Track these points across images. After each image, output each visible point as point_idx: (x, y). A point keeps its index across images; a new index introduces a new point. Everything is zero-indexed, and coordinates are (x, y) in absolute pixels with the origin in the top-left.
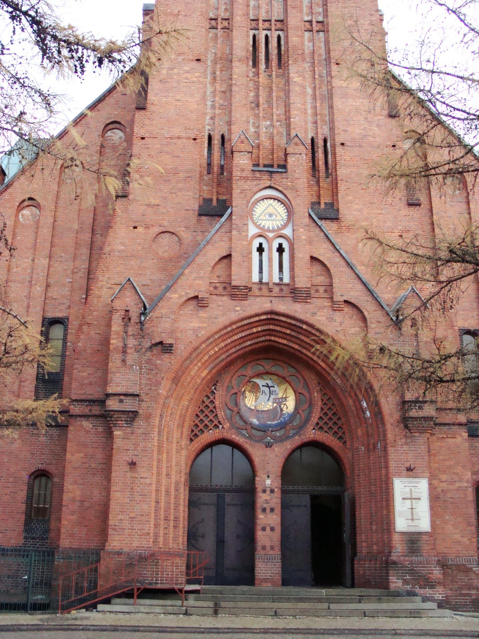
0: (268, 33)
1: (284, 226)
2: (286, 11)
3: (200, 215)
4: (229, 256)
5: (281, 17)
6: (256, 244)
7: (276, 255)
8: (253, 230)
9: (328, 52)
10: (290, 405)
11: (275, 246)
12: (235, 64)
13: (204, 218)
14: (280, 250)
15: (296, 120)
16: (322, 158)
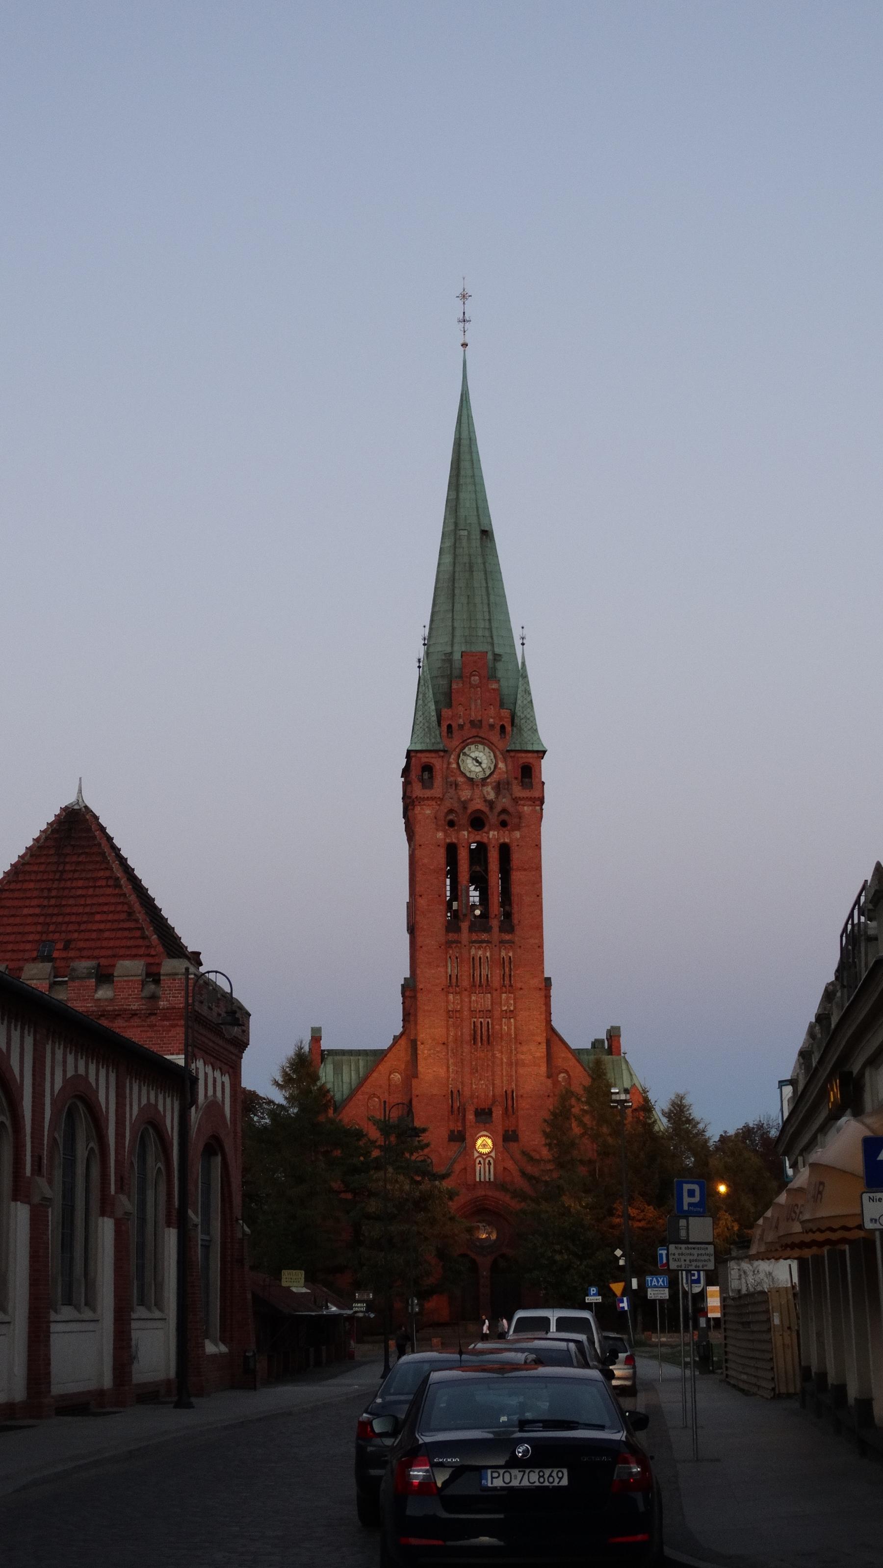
0: (482, 1020)
1: (491, 1152)
2: (492, 1004)
3: (450, 1140)
4: (465, 1169)
5: (490, 1008)
6: (477, 1161)
7: (487, 1166)
8: (476, 1155)
9: (516, 1035)
10: (494, 1237)
11: (487, 1162)
12: (465, 1046)
13: (452, 1143)
14: (489, 1163)
15: (498, 1082)
16: (509, 1100)
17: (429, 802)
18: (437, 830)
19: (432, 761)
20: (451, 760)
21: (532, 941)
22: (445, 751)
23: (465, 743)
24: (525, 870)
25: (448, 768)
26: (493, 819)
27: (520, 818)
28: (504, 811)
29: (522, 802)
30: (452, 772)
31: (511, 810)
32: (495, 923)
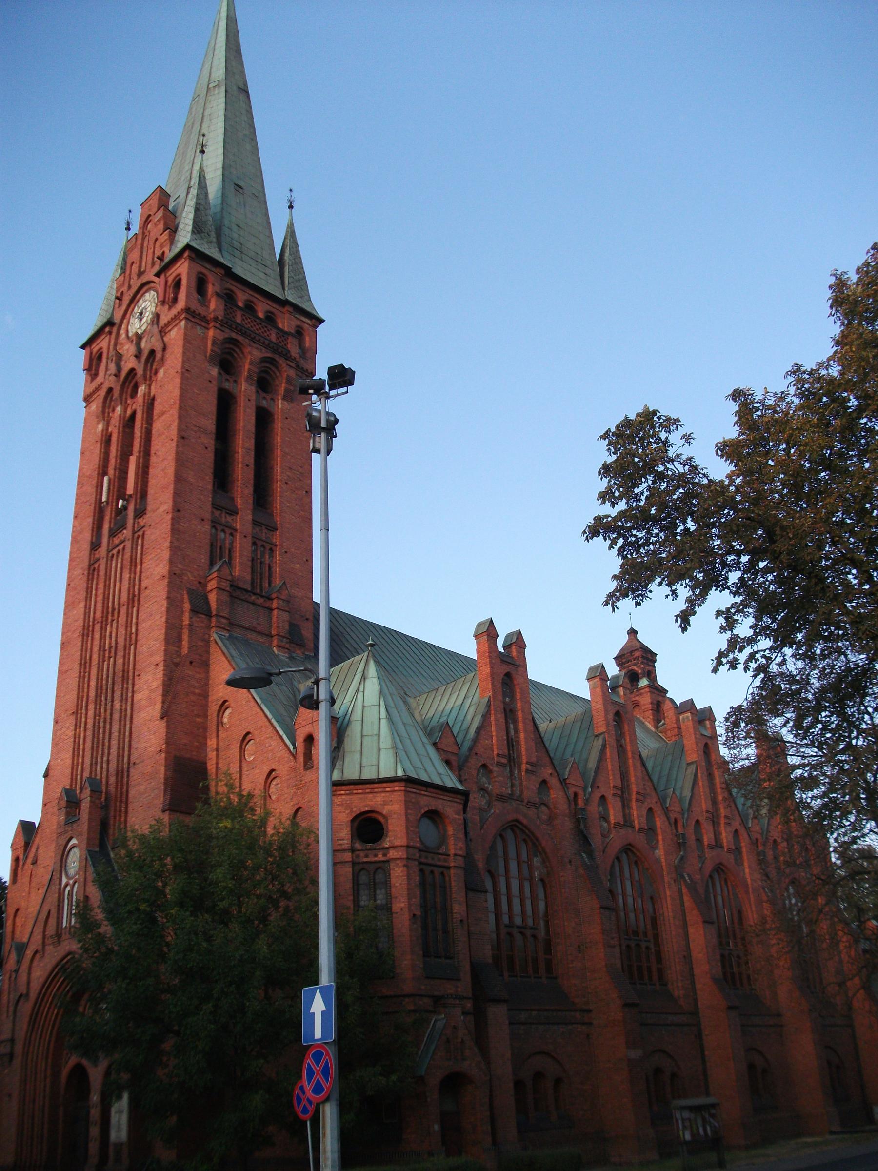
17: (95, 396)
18: (98, 423)
19: (101, 345)
20: (122, 331)
21: (161, 510)
22: (110, 323)
23: (133, 301)
24: (163, 413)
25: (116, 345)
26: (140, 372)
27: (164, 349)
28: (152, 352)
29: (169, 328)
30: (122, 344)
31: (158, 347)
32: (131, 508)
